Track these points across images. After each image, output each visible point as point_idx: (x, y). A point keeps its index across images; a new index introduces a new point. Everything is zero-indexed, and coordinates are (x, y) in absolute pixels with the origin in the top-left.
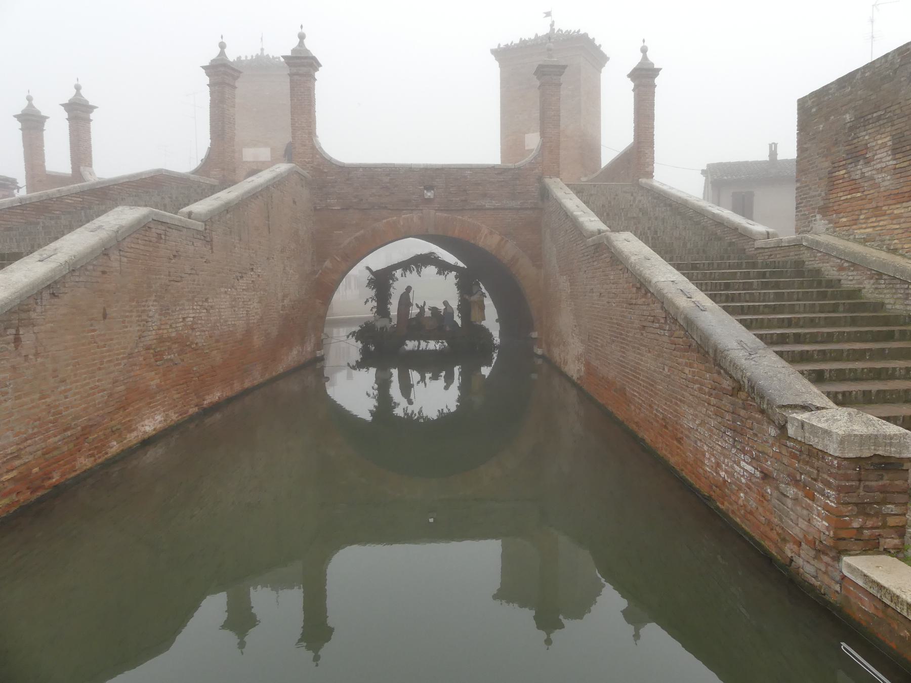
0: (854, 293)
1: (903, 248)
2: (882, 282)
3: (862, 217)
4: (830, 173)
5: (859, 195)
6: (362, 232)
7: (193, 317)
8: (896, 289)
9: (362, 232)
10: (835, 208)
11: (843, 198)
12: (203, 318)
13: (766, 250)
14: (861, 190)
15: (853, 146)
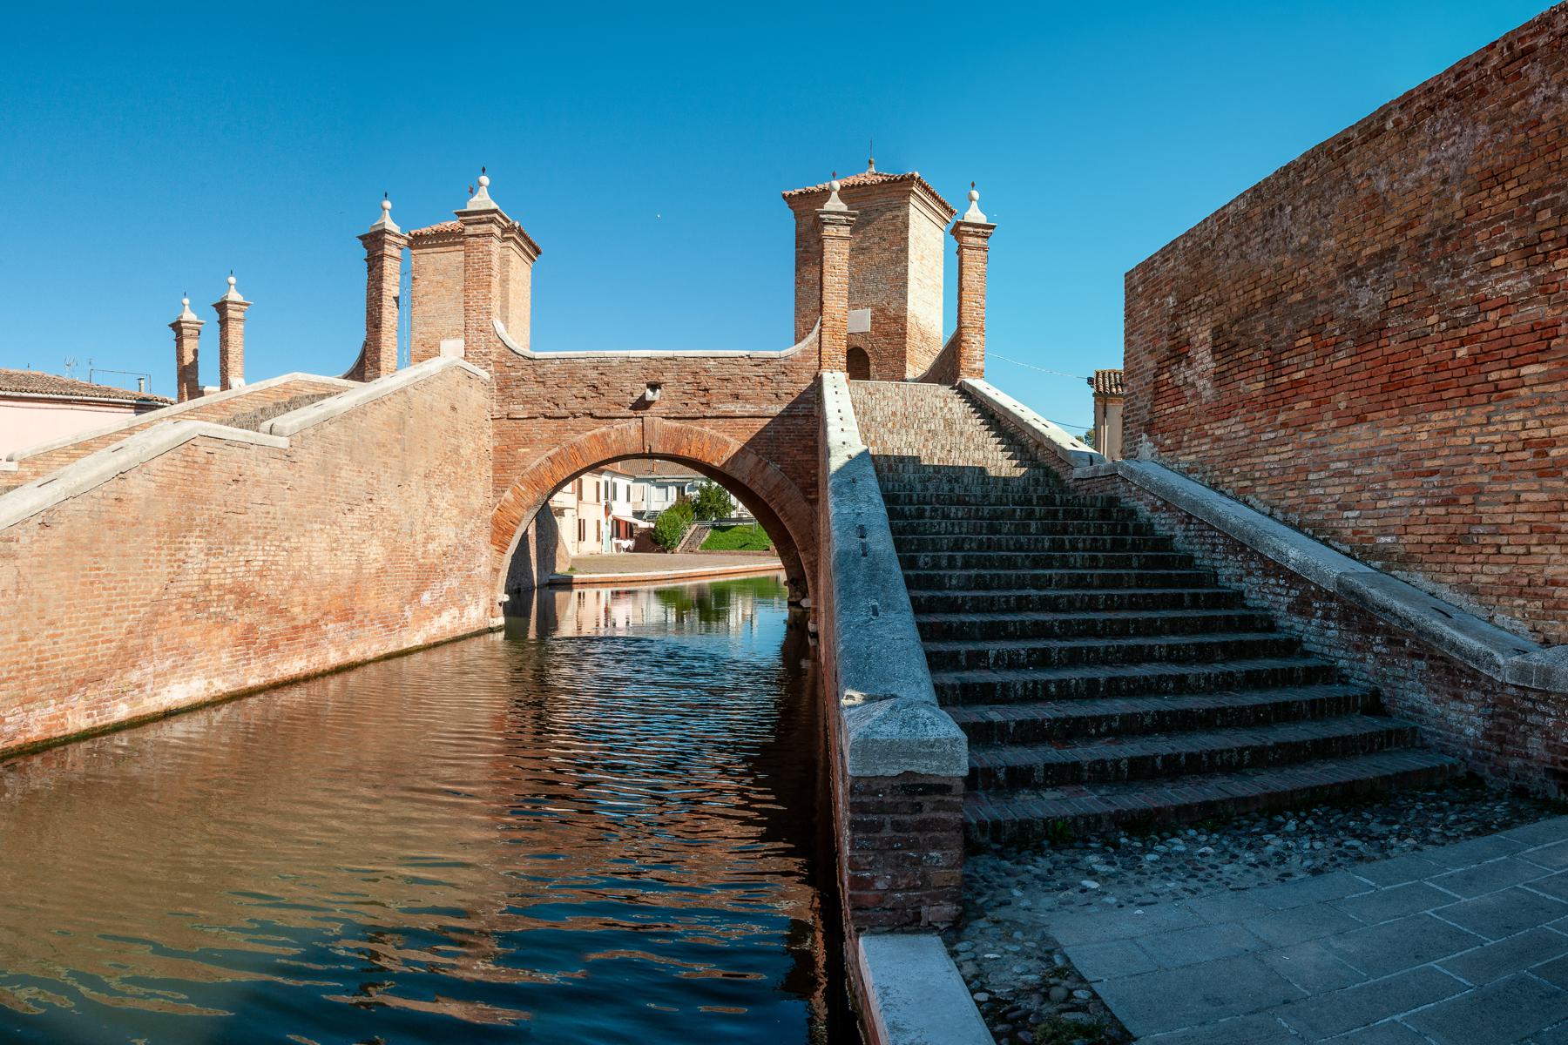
0: (1165, 542)
1: (1223, 482)
2: (1192, 527)
3: (1185, 438)
4: (1156, 376)
5: (1182, 407)
6: (557, 449)
7: (263, 561)
8: (1204, 537)
9: (557, 449)
10: (1160, 425)
11: (1168, 412)
12: (280, 562)
13: (1085, 482)
14: (1184, 401)
15: (1176, 341)
